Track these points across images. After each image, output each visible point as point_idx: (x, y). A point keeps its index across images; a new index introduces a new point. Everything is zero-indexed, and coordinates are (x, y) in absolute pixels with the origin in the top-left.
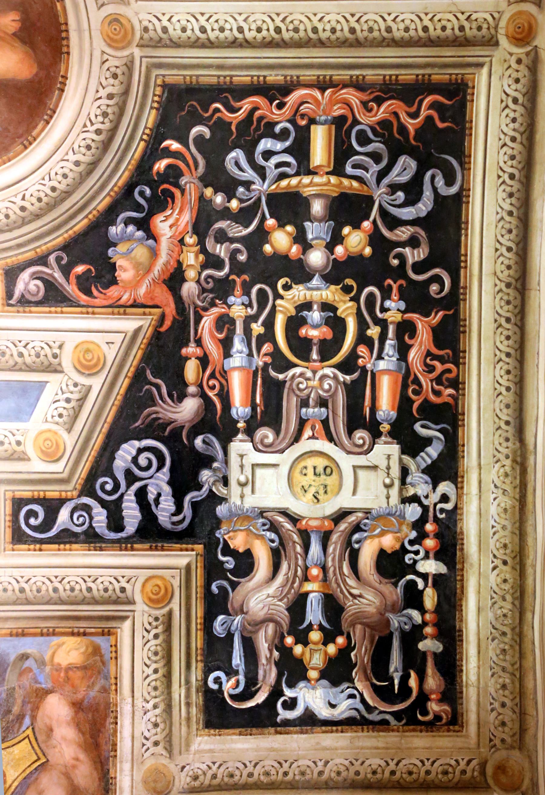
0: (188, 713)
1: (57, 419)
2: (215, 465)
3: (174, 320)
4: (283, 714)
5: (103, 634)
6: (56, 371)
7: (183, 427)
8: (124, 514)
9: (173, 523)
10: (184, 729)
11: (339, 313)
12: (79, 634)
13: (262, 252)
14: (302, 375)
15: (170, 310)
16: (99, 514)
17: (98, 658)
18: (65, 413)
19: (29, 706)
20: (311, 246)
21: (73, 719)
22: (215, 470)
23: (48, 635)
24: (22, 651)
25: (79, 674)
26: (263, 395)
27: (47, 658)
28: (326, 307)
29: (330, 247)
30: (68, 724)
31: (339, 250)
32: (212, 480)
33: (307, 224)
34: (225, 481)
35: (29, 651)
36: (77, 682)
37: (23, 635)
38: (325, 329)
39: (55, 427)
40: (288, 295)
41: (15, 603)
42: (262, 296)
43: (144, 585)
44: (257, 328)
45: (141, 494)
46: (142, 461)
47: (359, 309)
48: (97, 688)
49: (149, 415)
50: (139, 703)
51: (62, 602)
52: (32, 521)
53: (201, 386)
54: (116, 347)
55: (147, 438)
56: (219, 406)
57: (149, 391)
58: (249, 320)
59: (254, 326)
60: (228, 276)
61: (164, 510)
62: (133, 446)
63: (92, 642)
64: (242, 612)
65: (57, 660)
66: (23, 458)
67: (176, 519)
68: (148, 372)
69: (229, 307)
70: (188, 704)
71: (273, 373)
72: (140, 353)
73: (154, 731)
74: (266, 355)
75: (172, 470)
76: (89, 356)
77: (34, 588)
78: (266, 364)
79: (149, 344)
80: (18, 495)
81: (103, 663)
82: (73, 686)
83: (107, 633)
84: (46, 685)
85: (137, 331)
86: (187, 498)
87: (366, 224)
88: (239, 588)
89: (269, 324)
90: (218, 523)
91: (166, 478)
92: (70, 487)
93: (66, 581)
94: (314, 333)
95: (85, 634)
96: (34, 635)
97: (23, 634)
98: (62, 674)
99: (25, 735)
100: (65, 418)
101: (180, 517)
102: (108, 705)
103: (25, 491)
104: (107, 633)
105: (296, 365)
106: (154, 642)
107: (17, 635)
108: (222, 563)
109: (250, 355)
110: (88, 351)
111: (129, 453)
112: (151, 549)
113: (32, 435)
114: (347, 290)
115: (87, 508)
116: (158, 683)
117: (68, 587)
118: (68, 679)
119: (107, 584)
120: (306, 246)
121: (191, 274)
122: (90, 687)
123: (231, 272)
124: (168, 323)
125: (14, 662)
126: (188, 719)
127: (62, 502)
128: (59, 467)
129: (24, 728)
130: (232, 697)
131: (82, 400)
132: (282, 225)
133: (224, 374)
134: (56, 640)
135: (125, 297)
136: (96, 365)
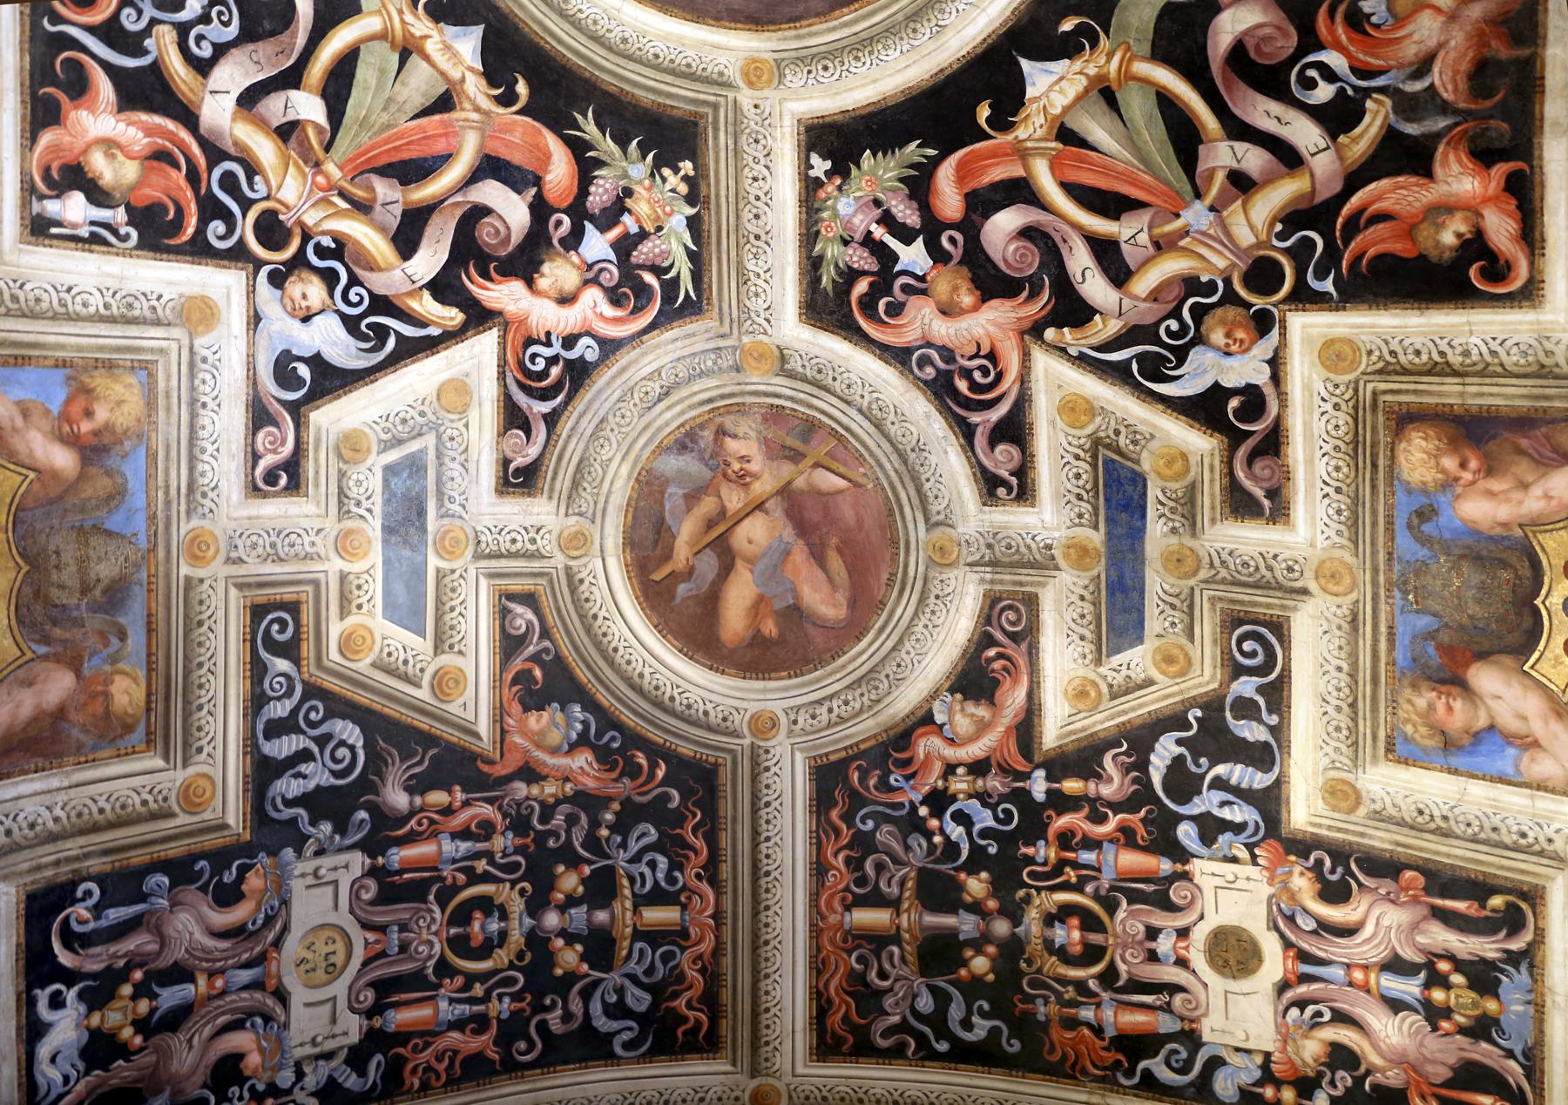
0: (46, 866)
1: (386, 650)
2: (337, 837)
3: (488, 775)
4: (43, 996)
5: (148, 733)
6: (436, 647)
7: (378, 795)
8: (285, 738)
9: (274, 799)
10: (26, 866)
11: (498, 950)
12: (148, 702)
13: (557, 863)
14: (433, 920)
15: (500, 770)
16: (283, 707)
17: (119, 731)
18: (393, 659)
19: (60, 649)
20: (563, 913)
21: (44, 712)
22: (331, 838)
23: (149, 663)
24: (129, 632)
25: (100, 711)
26: (412, 880)
27: (121, 666)
28: (503, 935)
29: (562, 933)
30: (38, 706)
31: (560, 943)
32: (321, 836)
33: (585, 908)
34: (319, 853)
35: (129, 641)
36: (90, 709)
37: (149, 631)
38: (481, 938)
39: (377, 648)
40: (515, 895)
41: (186, 616)
42: (511, 868)
43: (205, 775)
44: (482, 865)
45: (304, 756)
46: (342, 752)
47: (501, 971)
48: (83, 738)
49: (391, 755)
50: (61, 797)
51: (186, 676)
52: (276, 627)
53: (422, 810)
54: (459, 712)
55: (366, 755)
56: (401, 832)
57: (415, 754)
58: (489, 855)
59: (484, 862)
60: (533, 829)
61: (288, 784)
62: (357, 739)
63: (137, 722)
64: (172, 906)
65: (117, 678)
66: (344, 612)
67: (279, 801)
68: (435, 751)
69: (503, 833)
70: (57, 863)
71: (434, 889)
72: (455, 740)
73: (24, 825)
74: (454, 878)
75: (332, 788)
76: (451, 684)
77: (202, 638)
78: (442, 879)
79: (464, 749)
80: (304, 607)
81: (113, 740)
82: (86, 704)
83: (150, 741)
84: (87, 669)
85: (477, 735)
86: (301, 811)
87: (585, 967)
88: (201, 894)
89: (486, 878)
90: (274, 853)
91: (323, 783)
92: (313, 670)
93: (211, 677)
94: (476, 926)
95: (148, 710)
96: (149, 645)
97: (150, 630)
98: (100, 688)
99: (26, 649)
100: (387, 659)
101: (281, 806)
102: (60, 755)
103: (307, 616)
104: (150, 741)
105: (443, 912)
106: (137, 800)
107: (149, 623)
108: (229, 868)
109: (454, 861)
110: (457, 682)
111: (350, 736)
112: (245, 776)
113: (369, 622)
114: (520, 955)
115: (289, 693)
116: (86, 817)
117: (203, 680)
118: (94, 696)
119: (207, 728)
120: (562, 909)
121: (535, 790)
122: (84, 729)
123: (537, 832)
124: (486, 768)
125: (117, 624)
126: (39, 868)
127: (296, 661)
128: (334, 655)
129: (34, 647)
130: (67, 919)
131: (406, 678)
132: (584, 881)
133: (434, 835)
134: (141, 674)
135: (511, 721)
136: (442, 691)
